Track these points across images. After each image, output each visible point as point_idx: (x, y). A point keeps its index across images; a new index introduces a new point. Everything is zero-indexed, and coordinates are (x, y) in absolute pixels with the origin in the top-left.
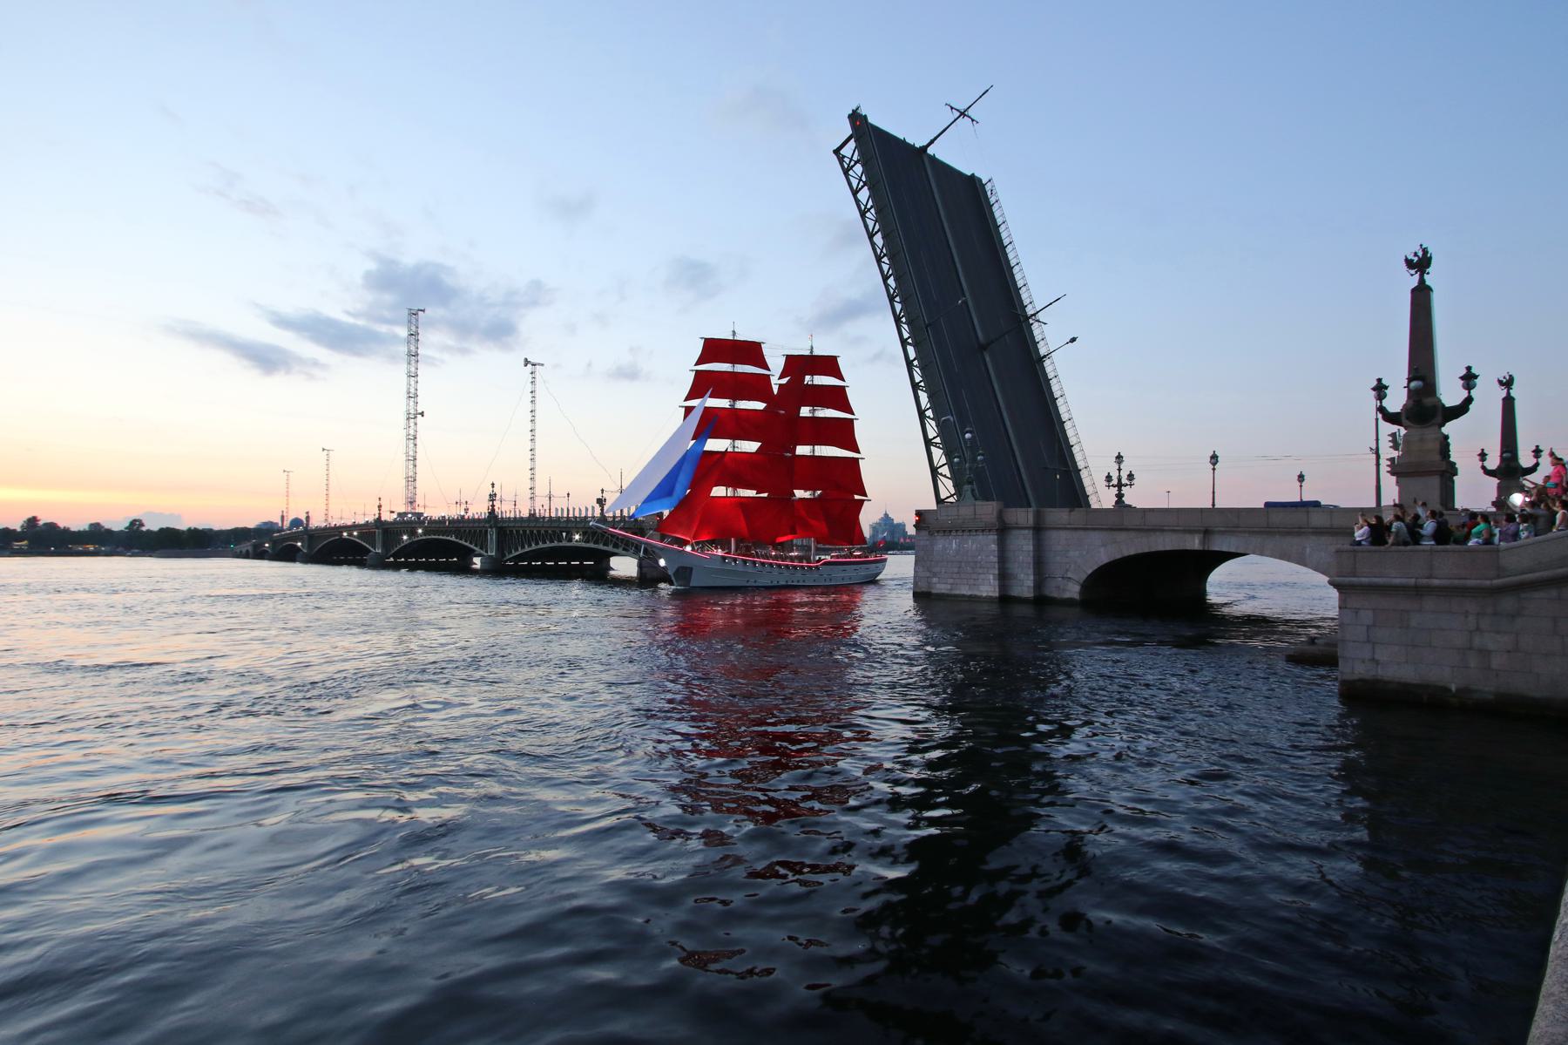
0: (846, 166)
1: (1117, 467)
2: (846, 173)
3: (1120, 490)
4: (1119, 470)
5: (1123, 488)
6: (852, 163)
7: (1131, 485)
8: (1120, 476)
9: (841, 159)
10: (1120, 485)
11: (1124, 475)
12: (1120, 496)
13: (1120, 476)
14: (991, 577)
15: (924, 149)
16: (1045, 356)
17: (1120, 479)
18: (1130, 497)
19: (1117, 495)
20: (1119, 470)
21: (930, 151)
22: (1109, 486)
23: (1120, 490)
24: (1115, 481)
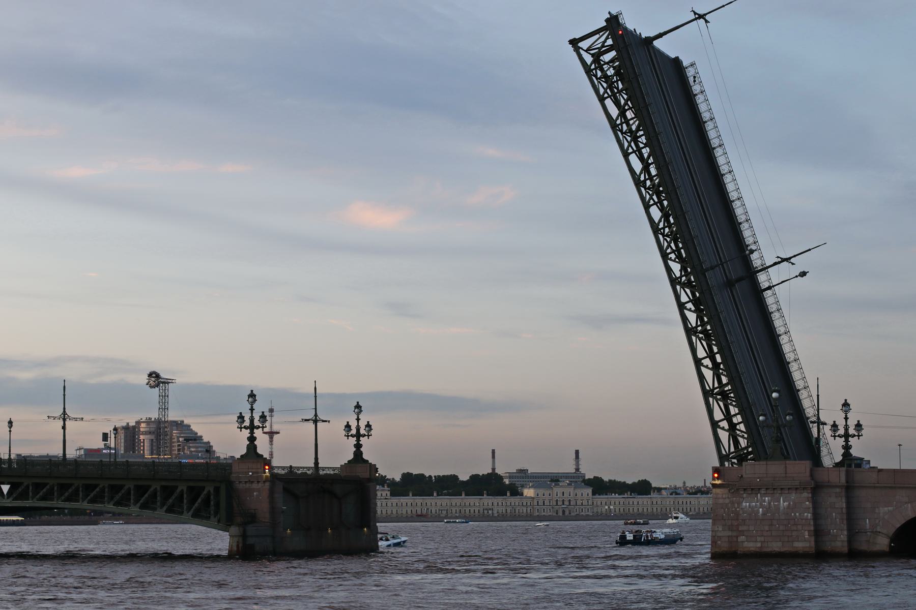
3: (847, 441)
4: (846, 418)
5: (850, 439)
7: (859, 436)
8: (846, 425)
10: (847, 436)
11: (852, 423)
12: (847, 447)
13: (846, 425)
14: (806, 533)
17: (846, 428)
19: (844, 447)
20: (846, 418)
22: (835, 436)
23: (847, 441)
24: (841, 431)
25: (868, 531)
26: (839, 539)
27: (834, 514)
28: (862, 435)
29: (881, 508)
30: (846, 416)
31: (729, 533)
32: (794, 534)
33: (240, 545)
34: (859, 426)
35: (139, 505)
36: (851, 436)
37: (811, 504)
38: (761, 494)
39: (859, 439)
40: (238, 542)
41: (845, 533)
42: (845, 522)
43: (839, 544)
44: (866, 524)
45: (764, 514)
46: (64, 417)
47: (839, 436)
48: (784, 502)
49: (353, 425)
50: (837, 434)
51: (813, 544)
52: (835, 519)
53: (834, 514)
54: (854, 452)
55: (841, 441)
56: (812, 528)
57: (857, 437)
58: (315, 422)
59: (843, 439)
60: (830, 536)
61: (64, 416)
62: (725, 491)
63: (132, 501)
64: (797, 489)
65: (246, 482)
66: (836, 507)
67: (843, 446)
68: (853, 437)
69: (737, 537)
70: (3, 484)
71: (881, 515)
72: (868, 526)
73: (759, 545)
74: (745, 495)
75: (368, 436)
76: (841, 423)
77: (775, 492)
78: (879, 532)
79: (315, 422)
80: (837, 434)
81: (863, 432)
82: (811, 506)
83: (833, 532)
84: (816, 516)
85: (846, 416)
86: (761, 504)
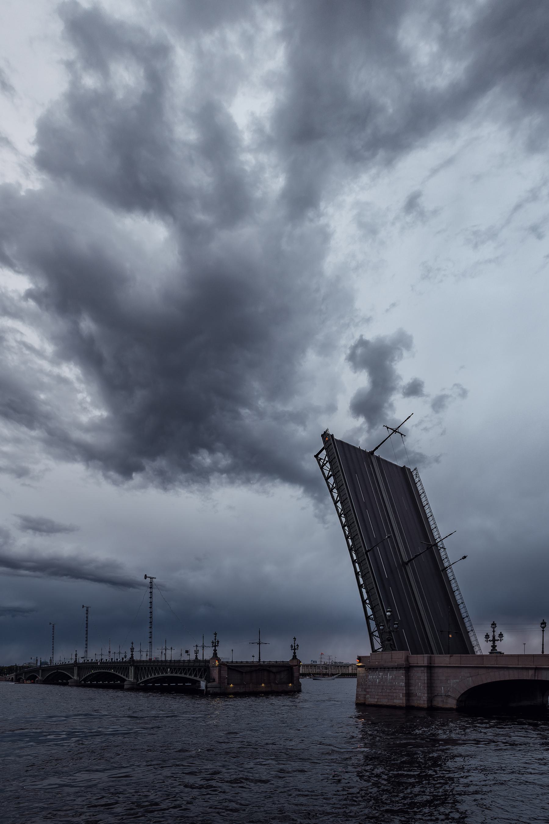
0: (321, 464)
2: (322, 468)
3: (494, 643)
6: (325, 462)
7: (501, 640)
8: (494, 635)
9: (319, 460)
10: (494, 640)
12: (494, 647)
13: (494, 635)
15: (372, 453)
16: (447, 567)
17: (494, 637)
18: (501, 647)
19: (492, 646)
21: (376, 453)
22: (487, 641)
23: (494, 643)
24: (491, 638)
25: (443, 694)
26: (422, 699)
27: (420, 684)
28: (503, 640)
29: (451, 680)
32: (395, 694)
36: (496, 640)
37: (404, 677)
38: (378, 671)
39: (501, 642)
41: (426, 695)
42: (426, 689)
43: (422, 702)
44: (442, 690)
45: (379, 683)
48: (390, 676)
50: (488, 640)
51: (404, 701)
52: (420, 686)
53: (420, 684)
55: (491, 643)
56: (404, 692)
57: (500, 641)
59: (492, 642)
60: (417, 697)
62: (364, 669)
64: (396, 668)
66: (421, 679)
67: (491, 646)
68: (498, 641)
71: (452, 684)
72: (443, 692)
74: (370, 672)
77: (385, 670)
78: (450, 696)
80: (488, 640)
82: (404, 678)
83: (419, 695)
86: (378, 677)
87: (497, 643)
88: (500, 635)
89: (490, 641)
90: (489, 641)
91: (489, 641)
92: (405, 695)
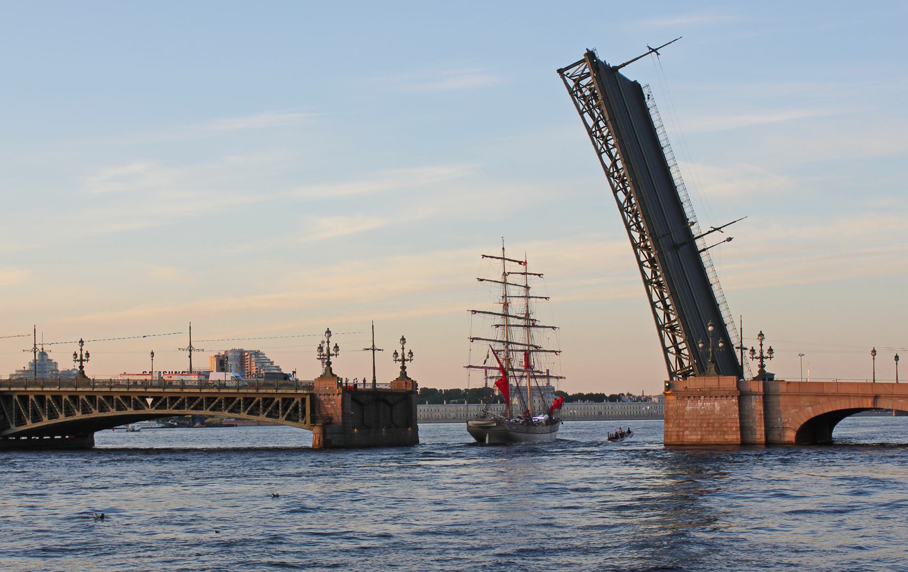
1: (759, 343)
3: (762, 361)
4: (761, 345)
5: (764, 360)
7: (771, 358)
8: (761, 350)
11: (765, 349)
12: (762, 366)
13: (761, 350)
17: (761, 352)
20: (761, 345)
22: (753, 358)
23: (762, 361)
24: (758, 354)
30: (761, 343)
31: (678, 429)
33: (321, 440)
34: (770, 350)
35: (247, 412)
40: (319, 438)
41: (763, 428)
42: (763, 420)
46: (190, 349)
47: (77, 360)
49: (400, 352)
51: (739, 437)
54: (767, 370)
55: (758, 362)
56: (739, 425)
58: (374, 350)
61: (190, 348)
63: (242, 409)
65: (324, 395)
68: (766, 358)
69: (683, 432)
70: (148, 397)
73: (699, 437)
75: (87, 360)
76: (757, 349)
77: (711, 398)
78: (788, 428)
79: (374, 350)
80: (754, 357)
81: (773, 355)
84: (742, 416)
85: (761, 343)
87: (766, 361)
88: (769, 350)
89: (757, 358)
90: (756, 358)
91: (756, 358)
92: (739, 429)
